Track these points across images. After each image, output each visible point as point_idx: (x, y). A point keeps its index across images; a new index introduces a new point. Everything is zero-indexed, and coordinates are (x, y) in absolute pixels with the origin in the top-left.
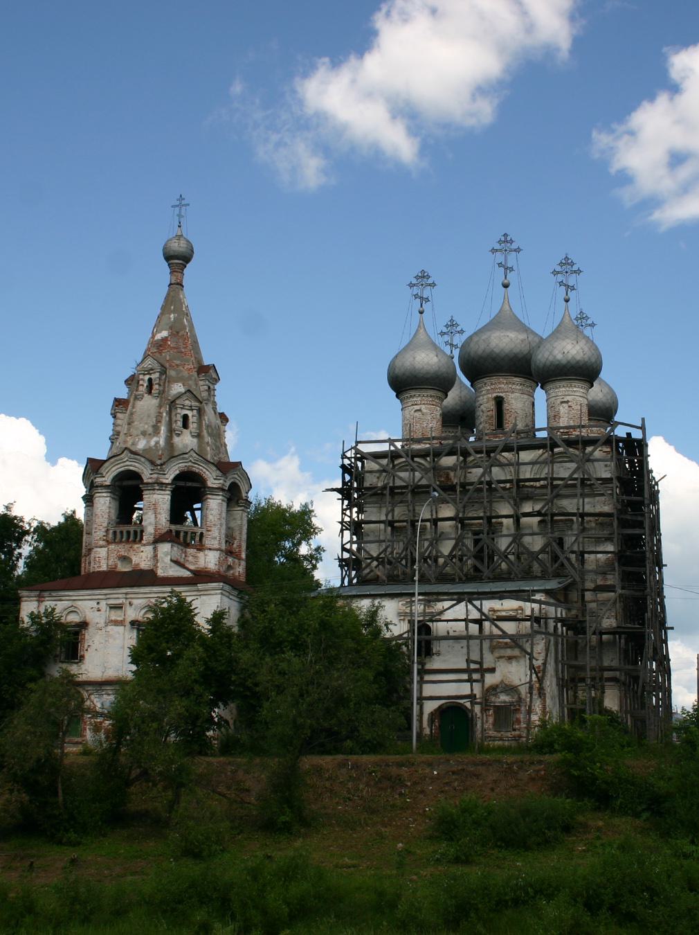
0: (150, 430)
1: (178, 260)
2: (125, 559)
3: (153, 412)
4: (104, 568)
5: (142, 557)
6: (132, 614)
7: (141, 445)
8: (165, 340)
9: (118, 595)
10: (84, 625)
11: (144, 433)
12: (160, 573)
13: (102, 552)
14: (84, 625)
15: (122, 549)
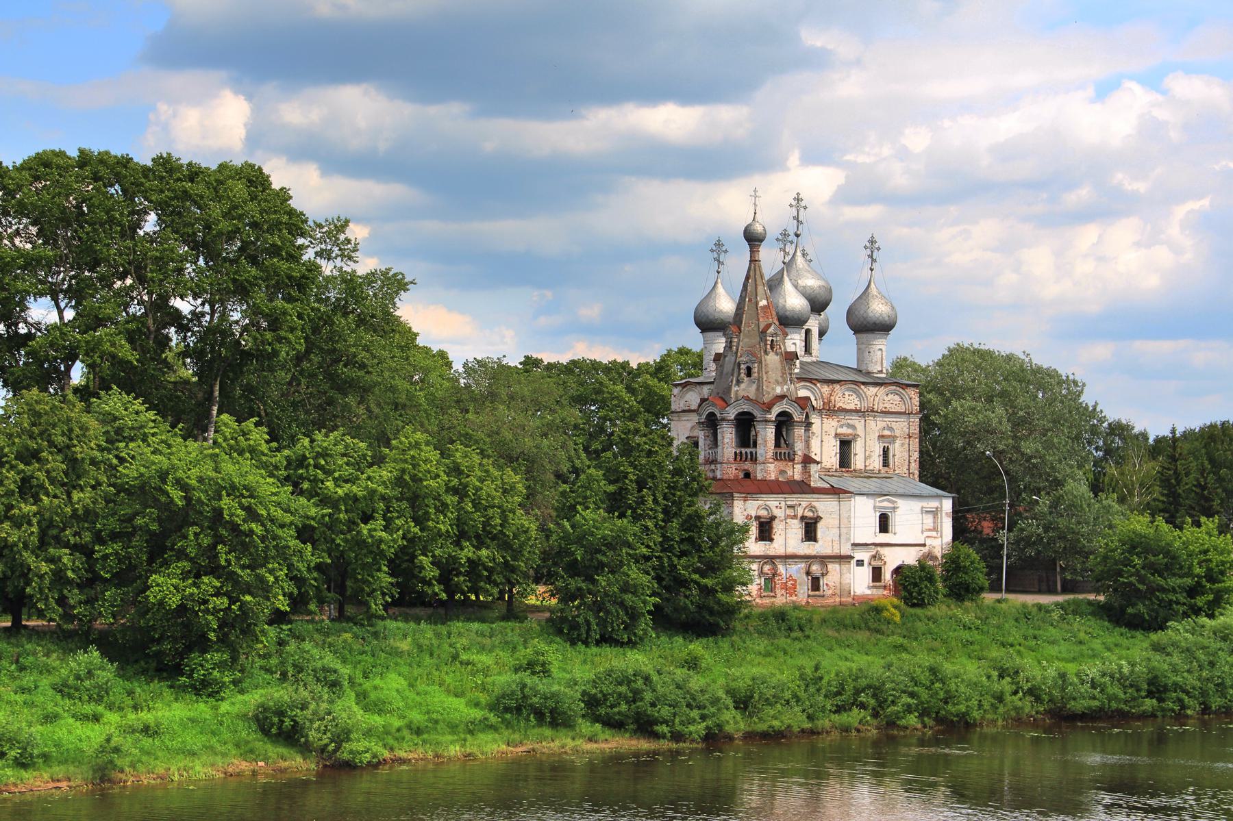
0: (780, 379)
1: (753, 239)
2: (782, 472)
3: (779, 366)
4: (773, 478)
5: (796, 472)
6: (800, 512)
7: (778, 390)
8: (765, 307)
9: (793, 499)
10: (773, 518)
11: (777, 382)
12: (813, 484)
13: (771, 467)
14: (773, 518)
15: (781, 465)
